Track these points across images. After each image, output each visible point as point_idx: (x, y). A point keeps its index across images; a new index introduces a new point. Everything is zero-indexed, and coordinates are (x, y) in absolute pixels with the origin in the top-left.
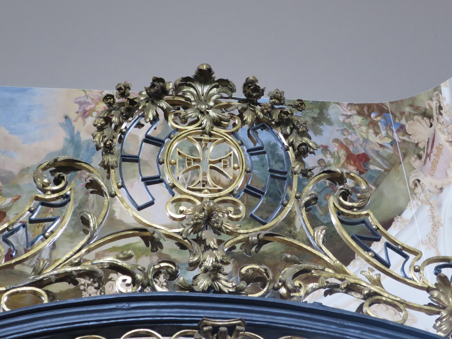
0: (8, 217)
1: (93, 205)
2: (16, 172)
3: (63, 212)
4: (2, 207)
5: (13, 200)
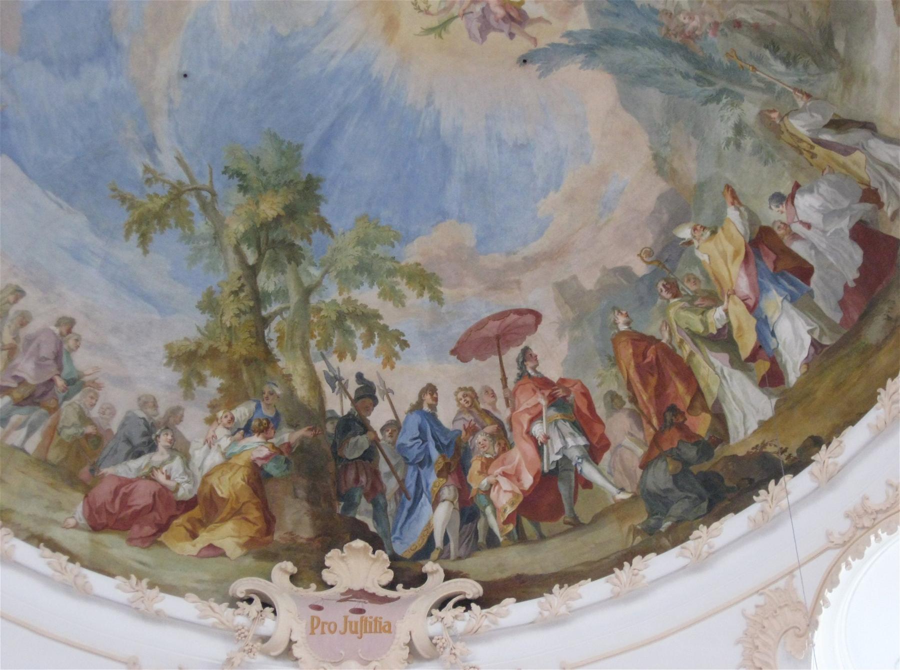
0: (774, 222)
1: (769, 13)
2: (661, 186)
3: (784, 89)
4: (746, 233)
5: (733, 204)
